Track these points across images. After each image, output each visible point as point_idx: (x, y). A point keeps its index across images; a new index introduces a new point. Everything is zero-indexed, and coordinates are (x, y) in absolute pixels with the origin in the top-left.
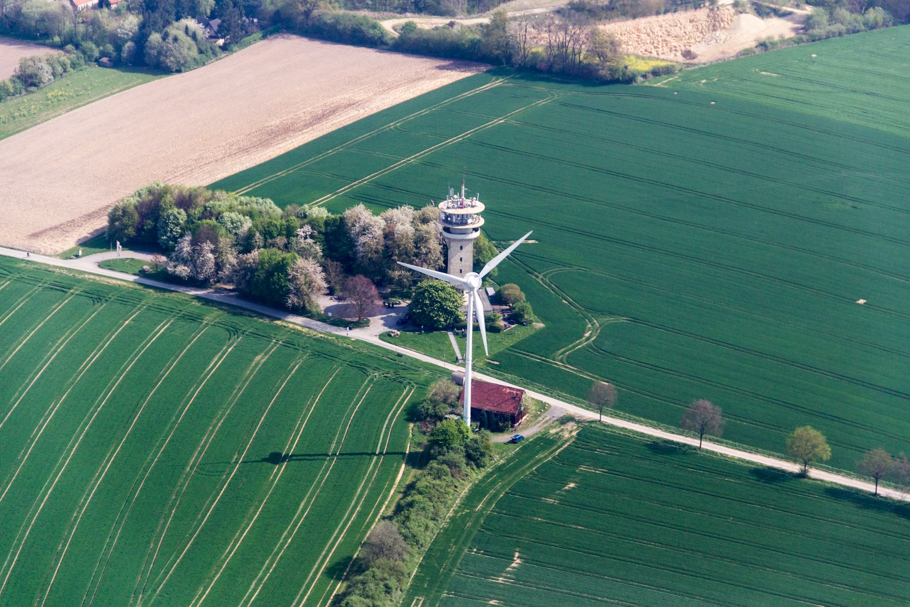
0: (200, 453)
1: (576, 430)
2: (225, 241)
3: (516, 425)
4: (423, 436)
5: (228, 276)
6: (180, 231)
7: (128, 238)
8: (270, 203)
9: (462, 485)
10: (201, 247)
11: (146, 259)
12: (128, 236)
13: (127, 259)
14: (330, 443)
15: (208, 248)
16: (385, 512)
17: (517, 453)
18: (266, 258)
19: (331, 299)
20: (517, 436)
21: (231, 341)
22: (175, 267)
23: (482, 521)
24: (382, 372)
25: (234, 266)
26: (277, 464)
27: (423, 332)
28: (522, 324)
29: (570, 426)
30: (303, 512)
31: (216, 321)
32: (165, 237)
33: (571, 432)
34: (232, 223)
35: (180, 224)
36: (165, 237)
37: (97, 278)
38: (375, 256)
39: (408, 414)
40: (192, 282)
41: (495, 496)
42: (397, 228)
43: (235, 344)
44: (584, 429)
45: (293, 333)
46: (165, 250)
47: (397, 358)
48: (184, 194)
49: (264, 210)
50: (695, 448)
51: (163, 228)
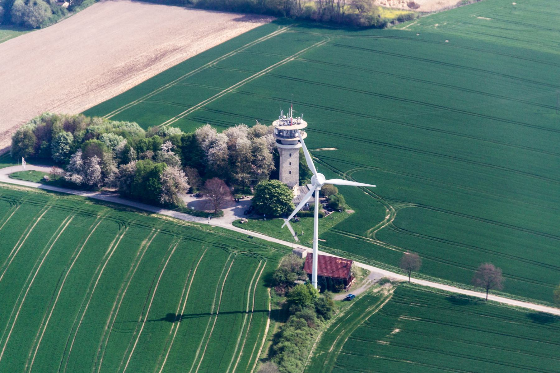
0: (113, 316)
1: (393, 289)
2: (108, 155)
3: (347, 287)
4: (279, 297)
5: (112, 182)
6: (69, 148)
7: (28, 155)
8: (136, 126)
9: (316, 333)
10: (90, 160)
11: (46, 171)
12: (29, 154)
13: (30, 171)
14: (211, 305)
15: (96, 161)
16: (262, 355)
17: (352, 308)
18: (142, 167)
19: (191, 197)
20: (350, 295)
21: (121, 230)
22: (71, 176)
23: (336, 360)
24: (239, 251)
25: (116, 173)
26: (173, 322)
27: (265, 219)
28: (337, 211)
29: (387, 286)
30: (200, 357)
31: (107, 215)
32: (58, 154)
33: (389, 291)
34: (110, 141)
35: (69, 143)
36: (58, 154)
37: (10, 186)
38: (223, 163)
39: (265, 281)
40: (85, 187)
41: (341, 340)
42: (237, 141)
43: (124, 233)
44: (398, 288)
45: (167, 223)
46: (61, 164)
47: (249, 239)
48: (70, 121)
49: (132, 131)
50: (483, 300)
51: (56, 147)
